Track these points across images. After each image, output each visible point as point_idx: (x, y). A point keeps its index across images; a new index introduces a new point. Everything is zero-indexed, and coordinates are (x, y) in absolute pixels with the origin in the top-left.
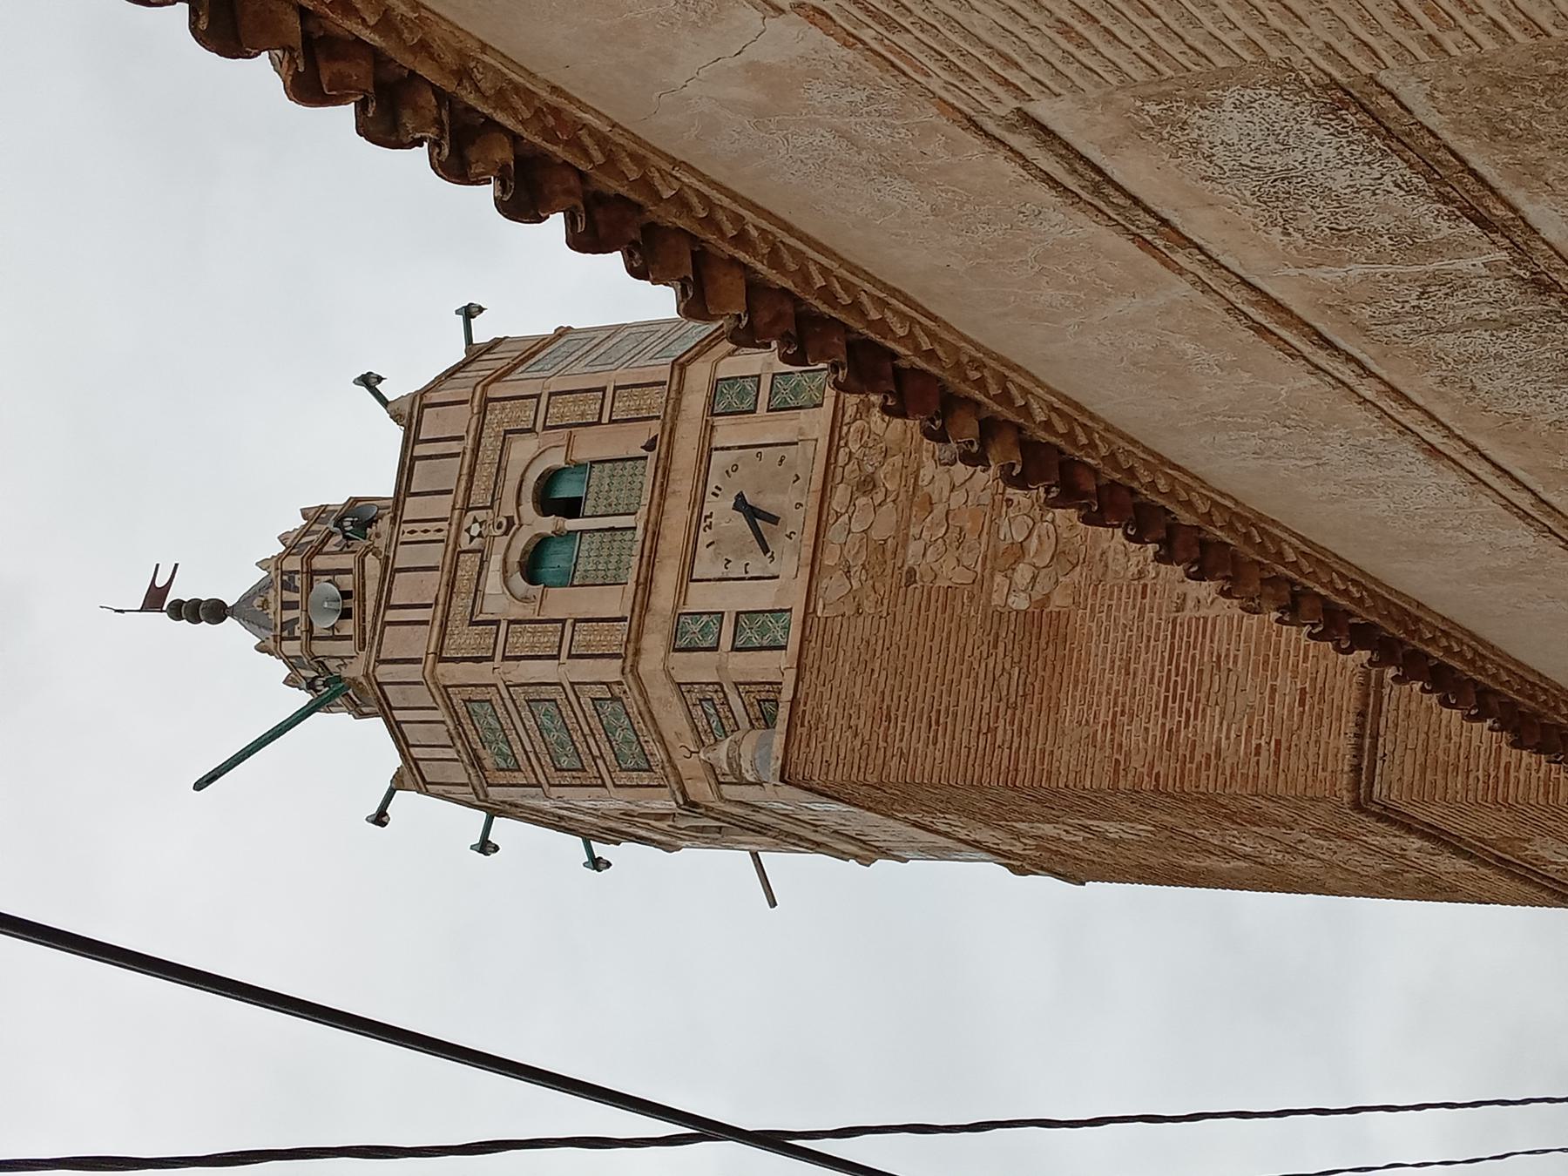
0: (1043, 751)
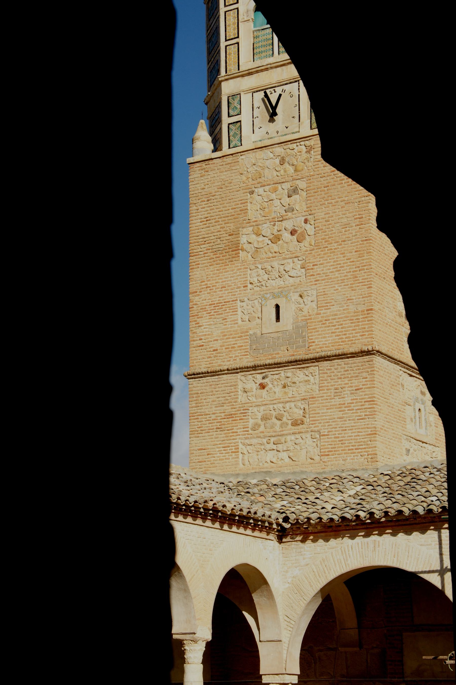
0: (199, 264)
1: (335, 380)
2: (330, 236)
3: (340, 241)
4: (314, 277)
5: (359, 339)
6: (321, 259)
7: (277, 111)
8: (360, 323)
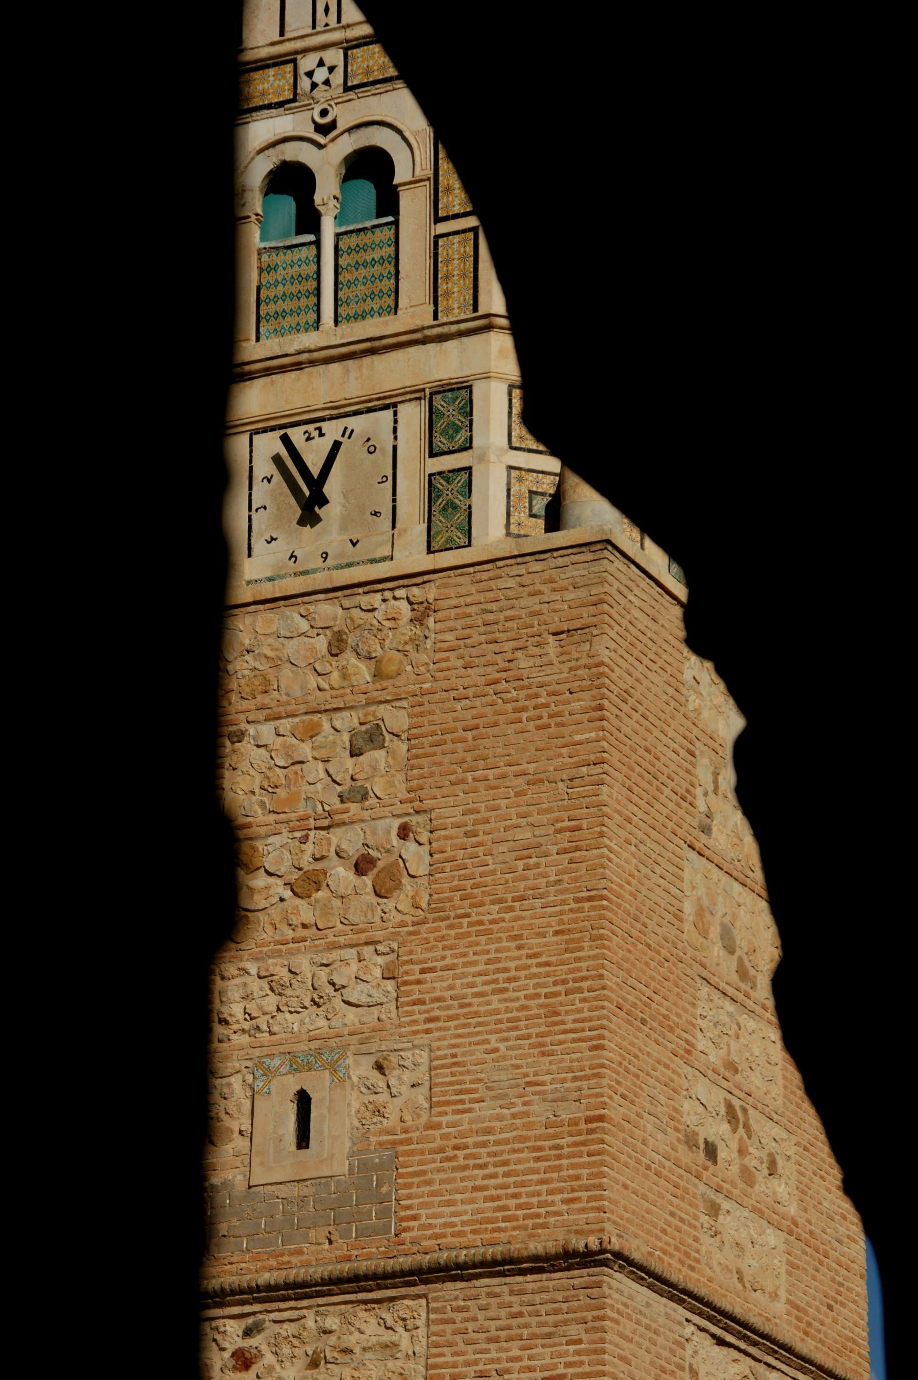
1: (478, 1346)
2: (479, 880)
3: (509, 896)
4: (424, 1007)
5: (558, 1214)
6: (448, 953)
7: (327, 490)
8: (565, 1162)
